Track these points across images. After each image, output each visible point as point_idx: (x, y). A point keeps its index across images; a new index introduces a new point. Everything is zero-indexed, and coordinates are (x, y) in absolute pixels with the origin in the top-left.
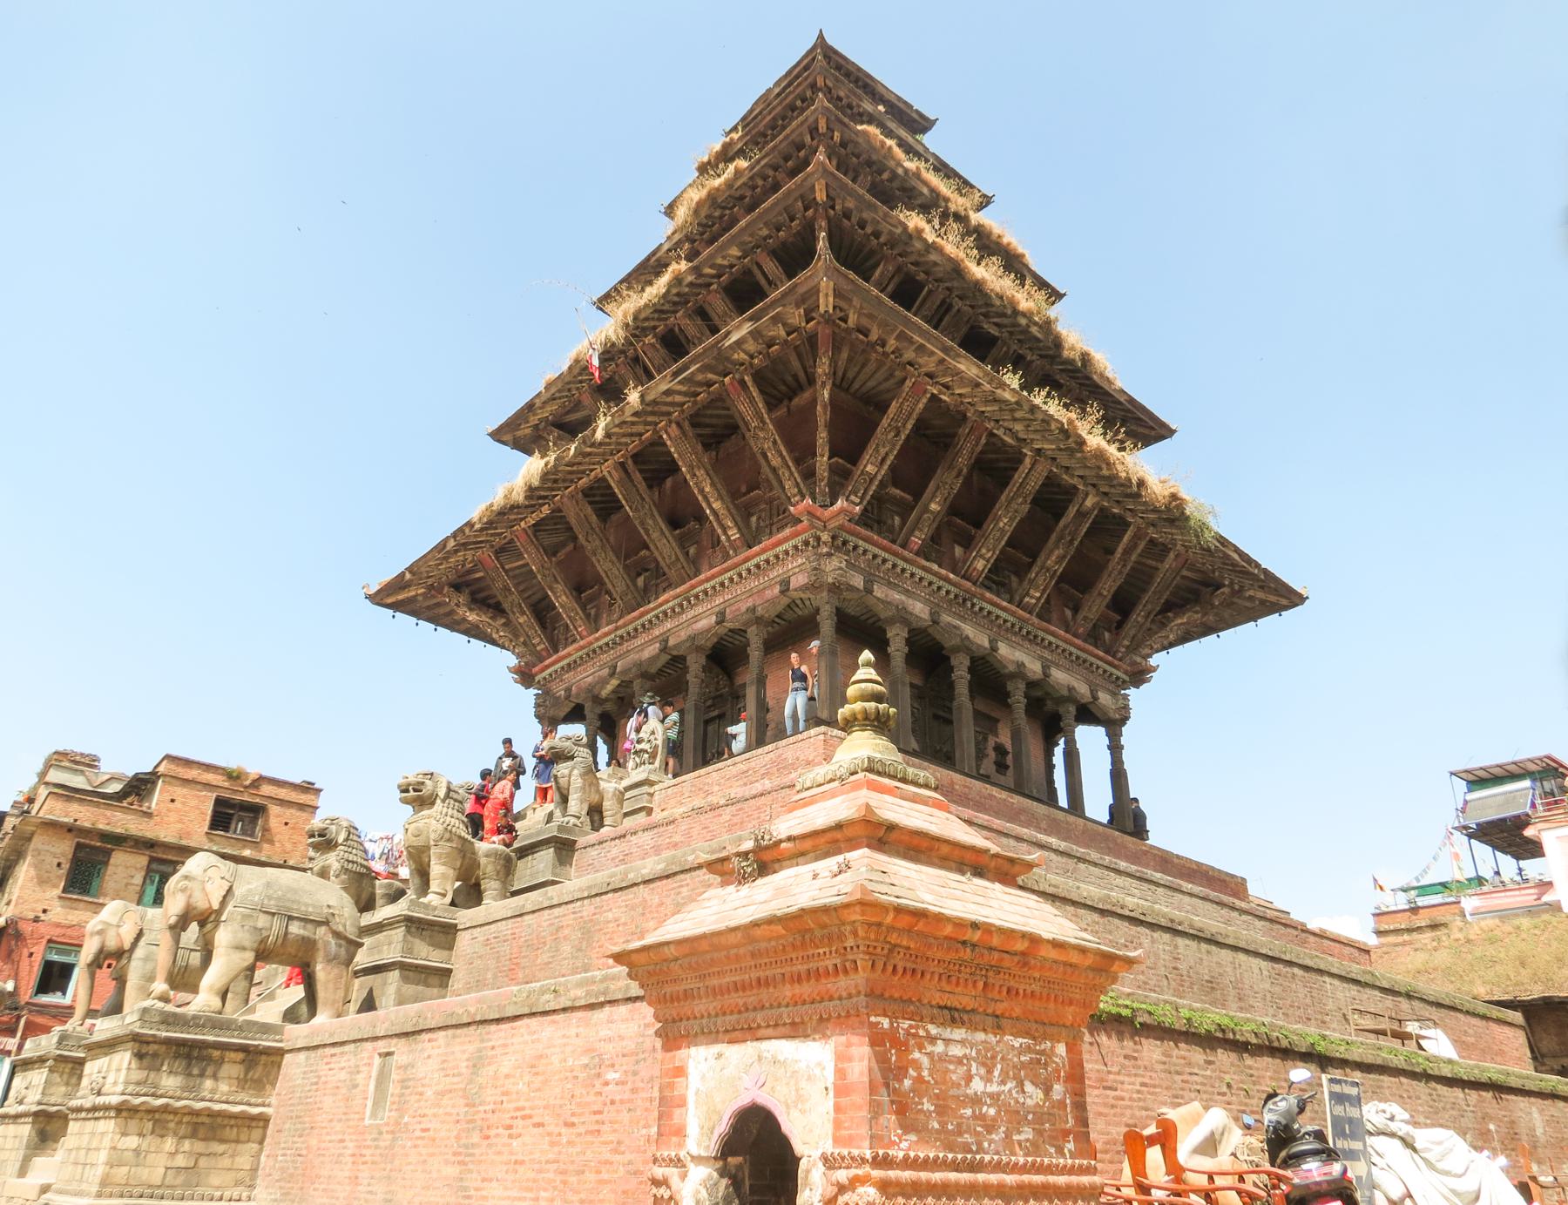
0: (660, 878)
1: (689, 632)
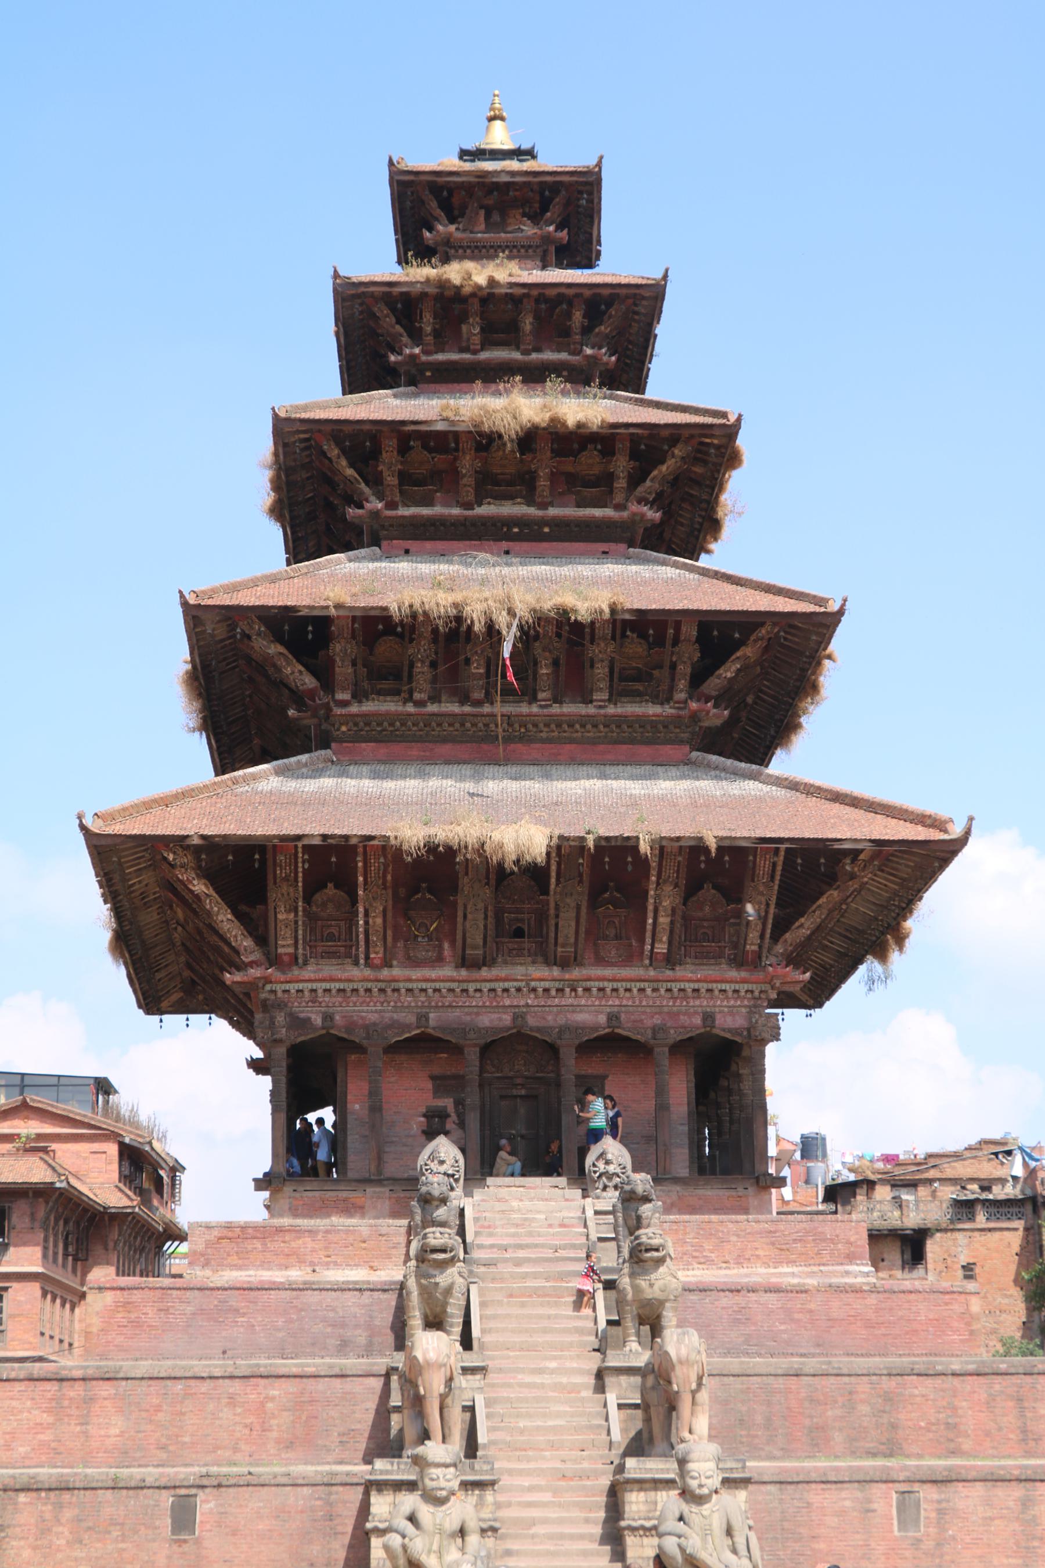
0: (971, 1375)
1: (561, 1020)
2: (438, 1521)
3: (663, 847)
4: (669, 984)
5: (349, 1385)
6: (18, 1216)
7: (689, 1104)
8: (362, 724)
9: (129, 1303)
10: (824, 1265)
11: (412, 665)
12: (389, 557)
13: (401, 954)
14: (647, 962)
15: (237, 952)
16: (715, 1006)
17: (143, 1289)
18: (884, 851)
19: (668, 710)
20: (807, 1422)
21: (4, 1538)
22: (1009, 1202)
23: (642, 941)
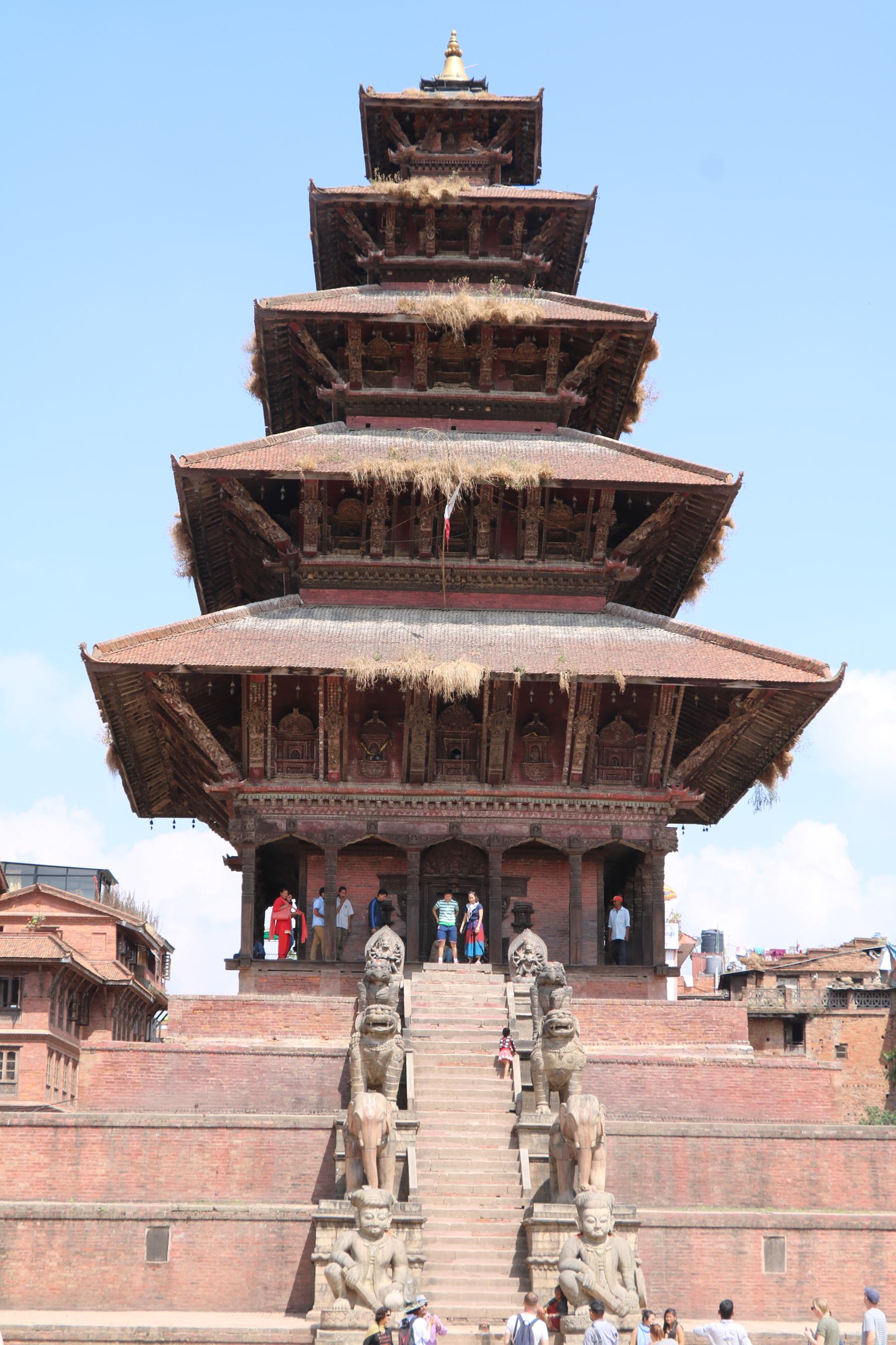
0: (831, 1139)
1: (491, 830)
2: (372, 1254)
3: (580, 684)
4: (583, 801)
5: (301, 1136)
6: (30, 986)
7: (598, 904)
8: (326, 573)
10: (709, 1043)
11: (369, 524)
12: (352, 430)
13: (354, 771)
14: (565, 781)
15: (215, 766)
16: (622, 821)
17: (128, 1051)
18: (770, 691)
19: (589, 566)
20: (691, 1176)
21: (5, 1259)
22: (877, 993)
23: (561, 764)
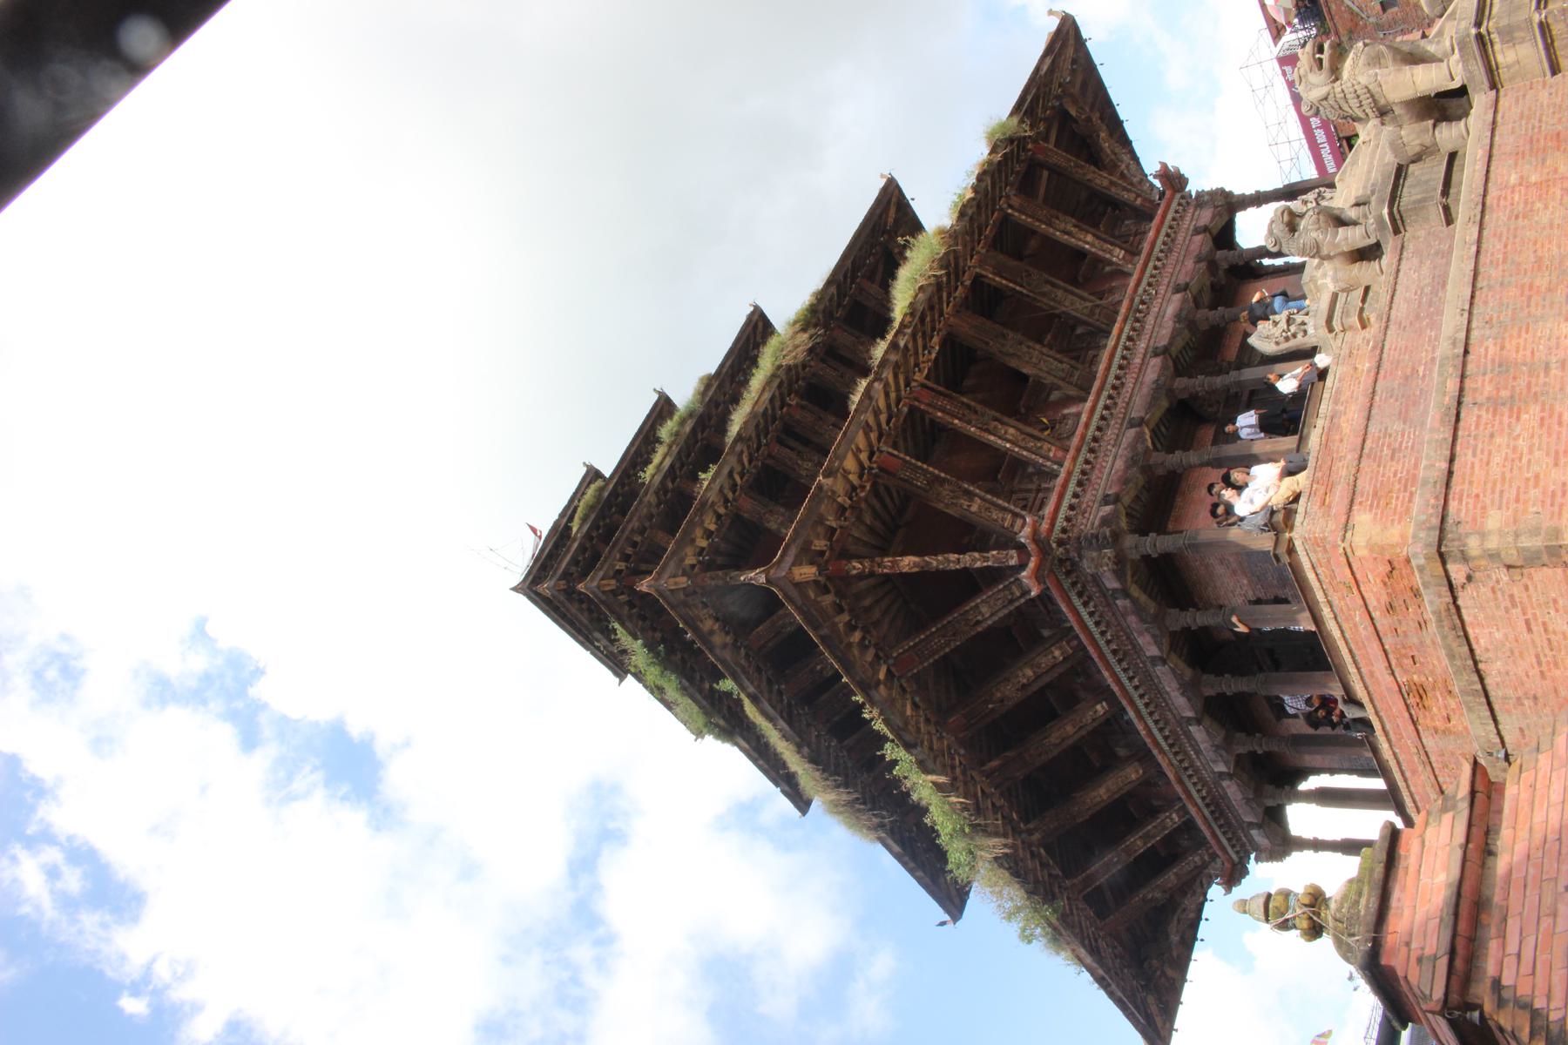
9: (1375, 494)
